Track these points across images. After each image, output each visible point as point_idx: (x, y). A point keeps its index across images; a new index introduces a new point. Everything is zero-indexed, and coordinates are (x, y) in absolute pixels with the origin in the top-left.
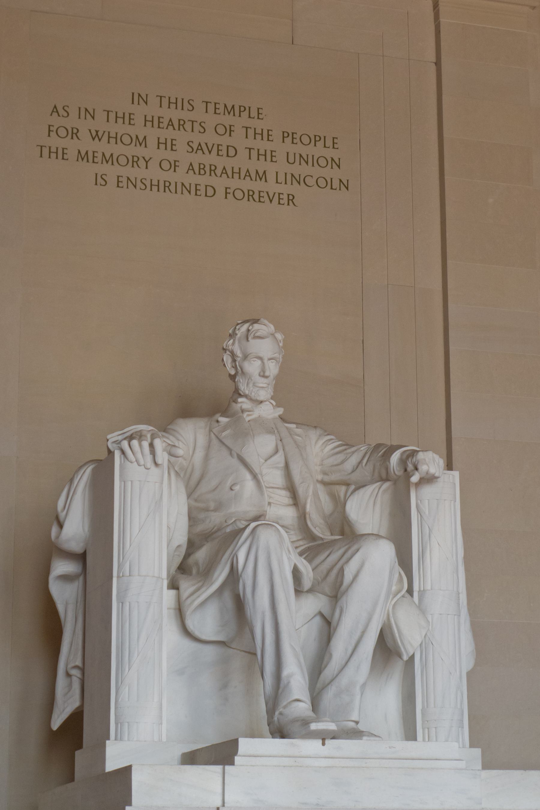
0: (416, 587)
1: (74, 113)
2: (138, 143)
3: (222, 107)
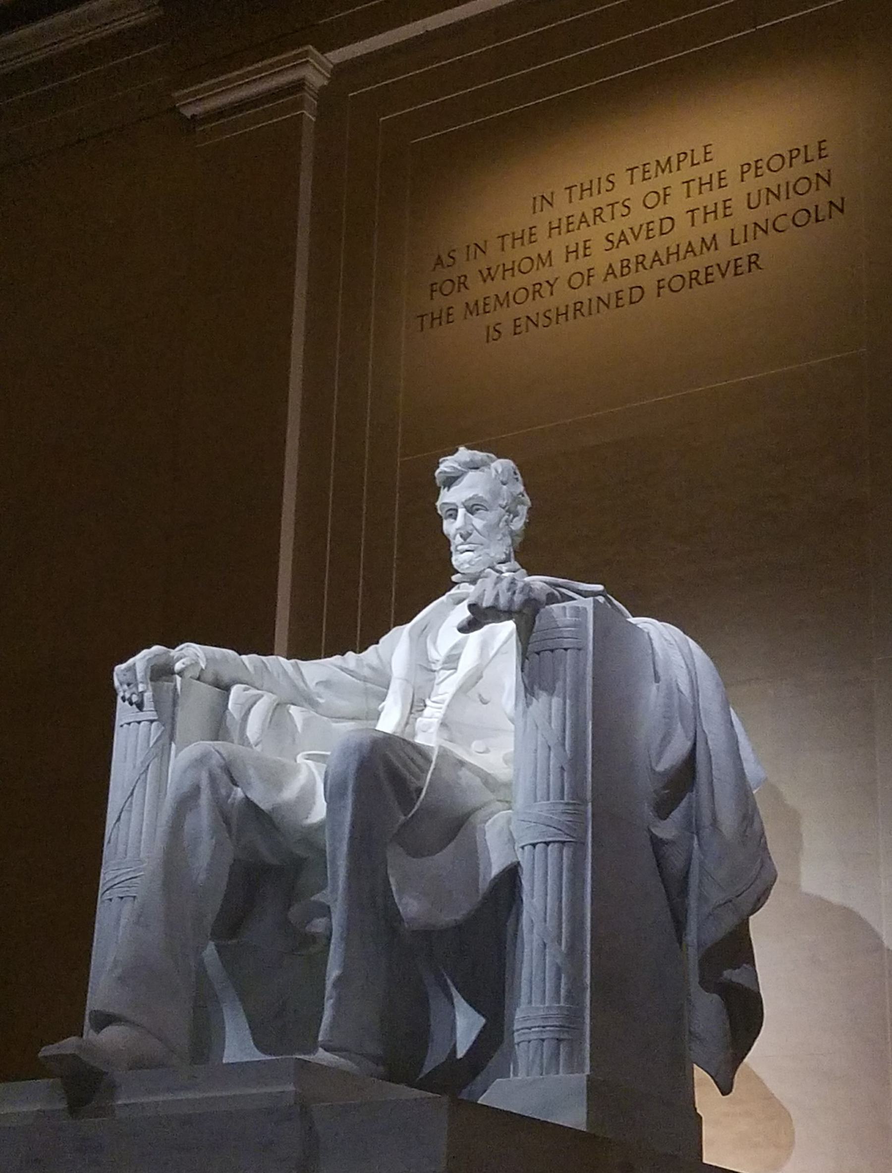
2: (541, 265)
3: (652, 167)
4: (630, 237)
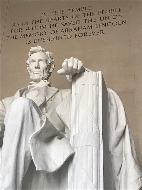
0: (72, 135)
1: (20, 24)
4: (68, 24)
